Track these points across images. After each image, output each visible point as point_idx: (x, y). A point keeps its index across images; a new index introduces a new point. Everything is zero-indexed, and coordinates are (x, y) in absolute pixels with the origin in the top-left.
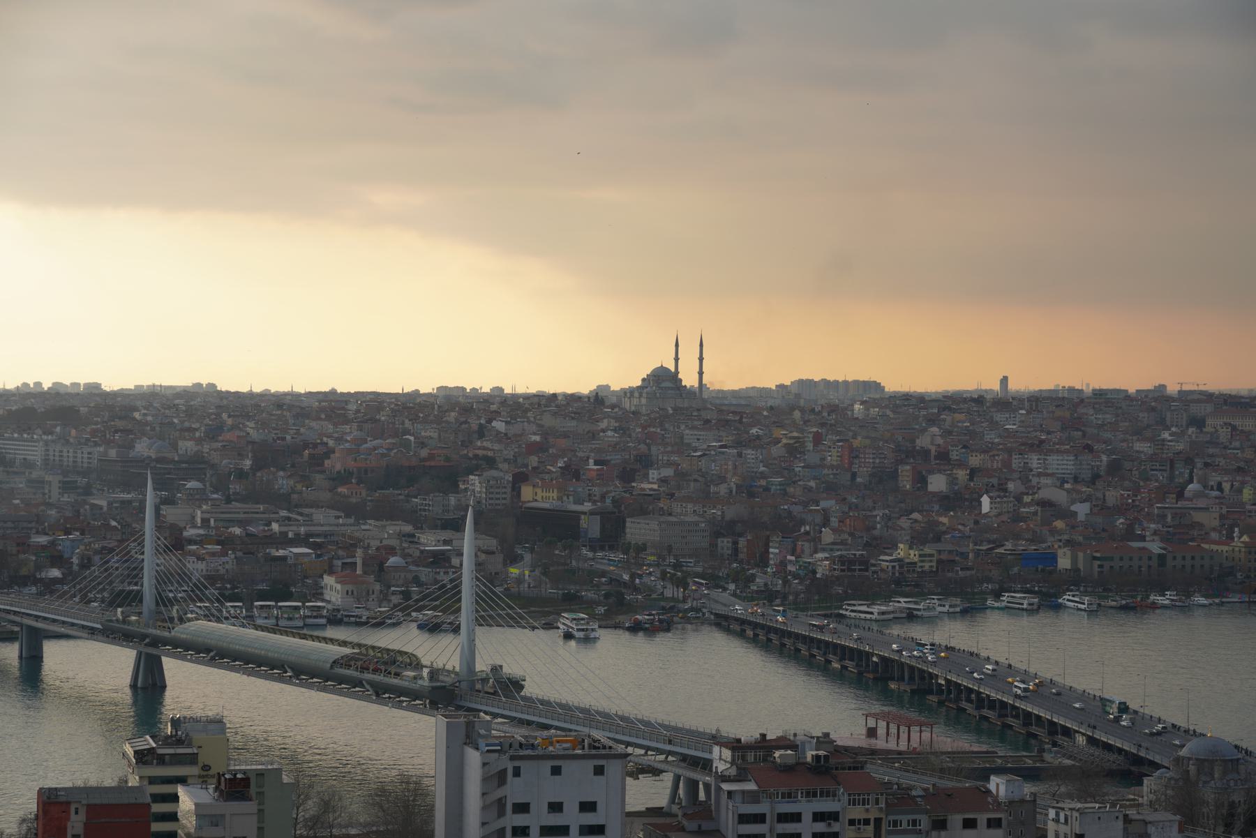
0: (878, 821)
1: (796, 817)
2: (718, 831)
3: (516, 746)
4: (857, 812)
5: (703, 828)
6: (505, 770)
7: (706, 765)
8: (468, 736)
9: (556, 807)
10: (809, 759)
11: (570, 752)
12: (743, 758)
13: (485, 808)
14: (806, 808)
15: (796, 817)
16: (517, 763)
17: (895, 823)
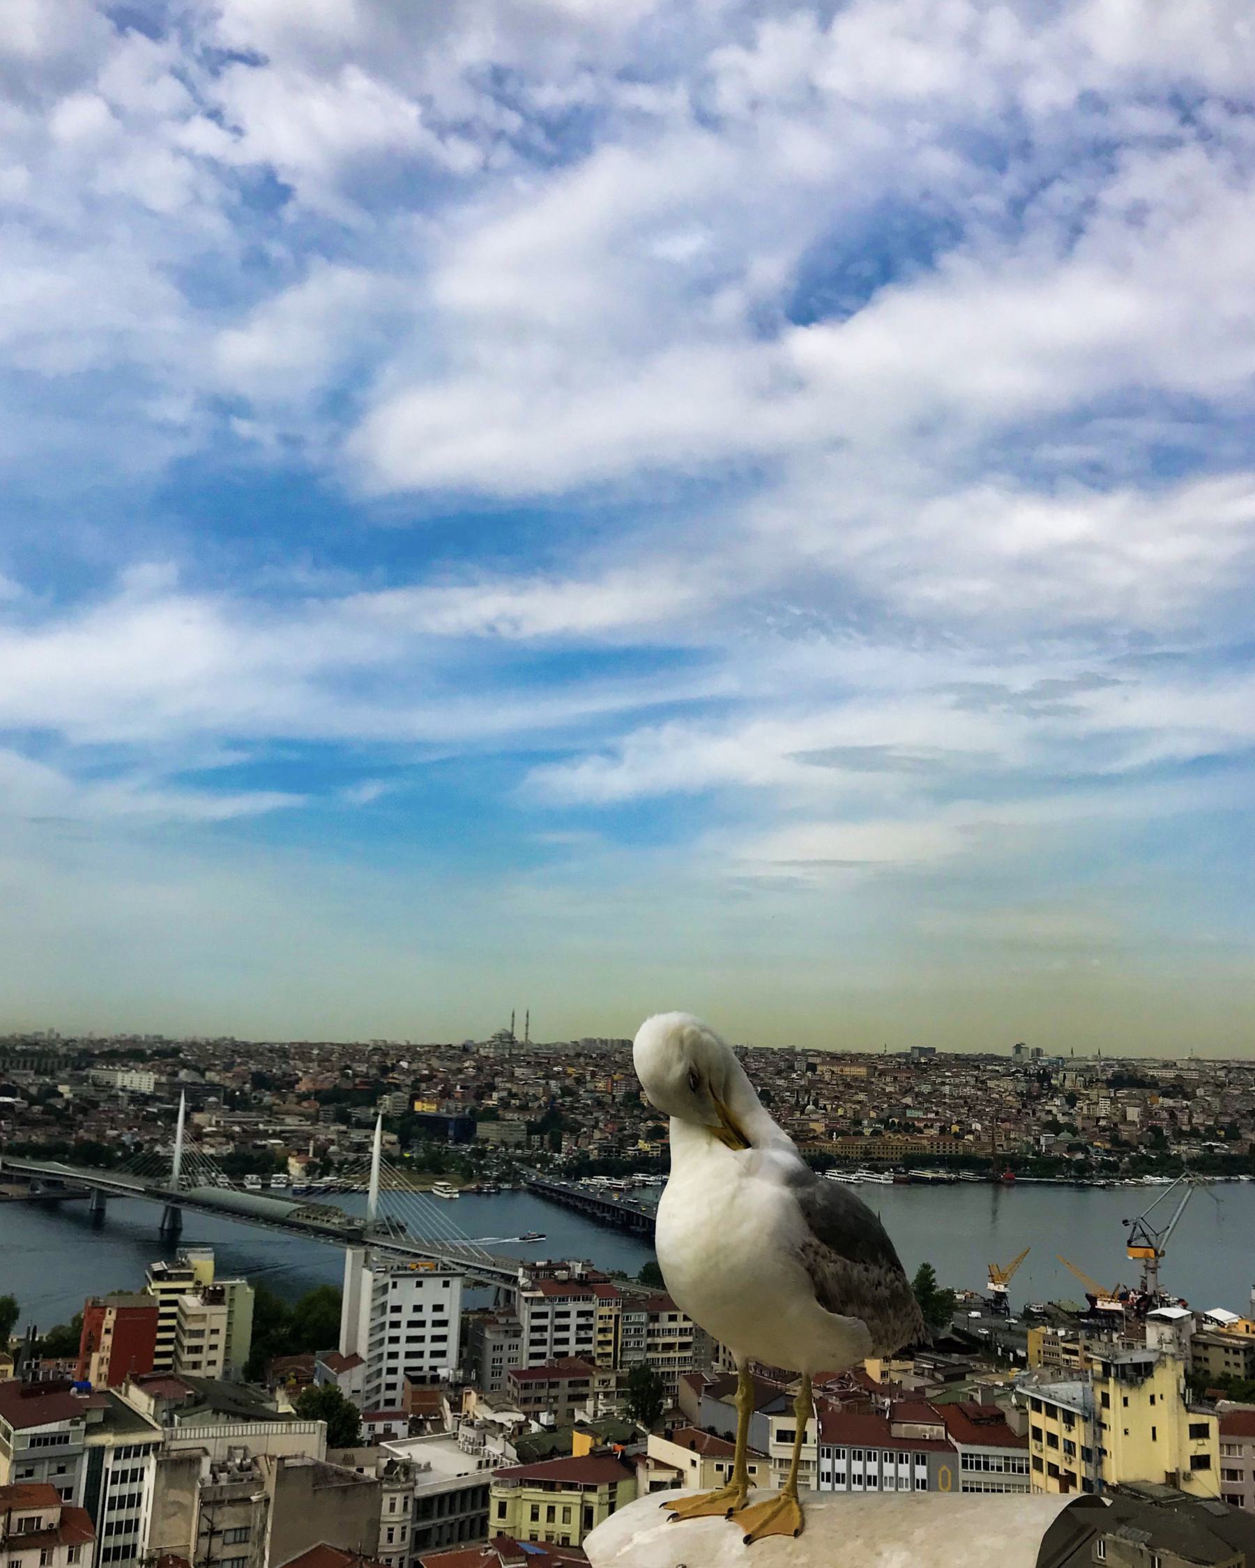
0: (617, 1317)
1: (566, 1314)
2: (519, 1323)
3: (395, 1268)
4: (605, 1311)
5: (510, 1321)
6: (387, 1284)
7: (515, 1280)
8: (366, 1261)
9: (418, 1308)
10: (576, 1277)
11: (429, 1272)
12: (537, 1276)
13: (373, 1309)
14: (573, 1307)
15: (566, 1314)
16: (395, 1280)
17: (627, 1317)
